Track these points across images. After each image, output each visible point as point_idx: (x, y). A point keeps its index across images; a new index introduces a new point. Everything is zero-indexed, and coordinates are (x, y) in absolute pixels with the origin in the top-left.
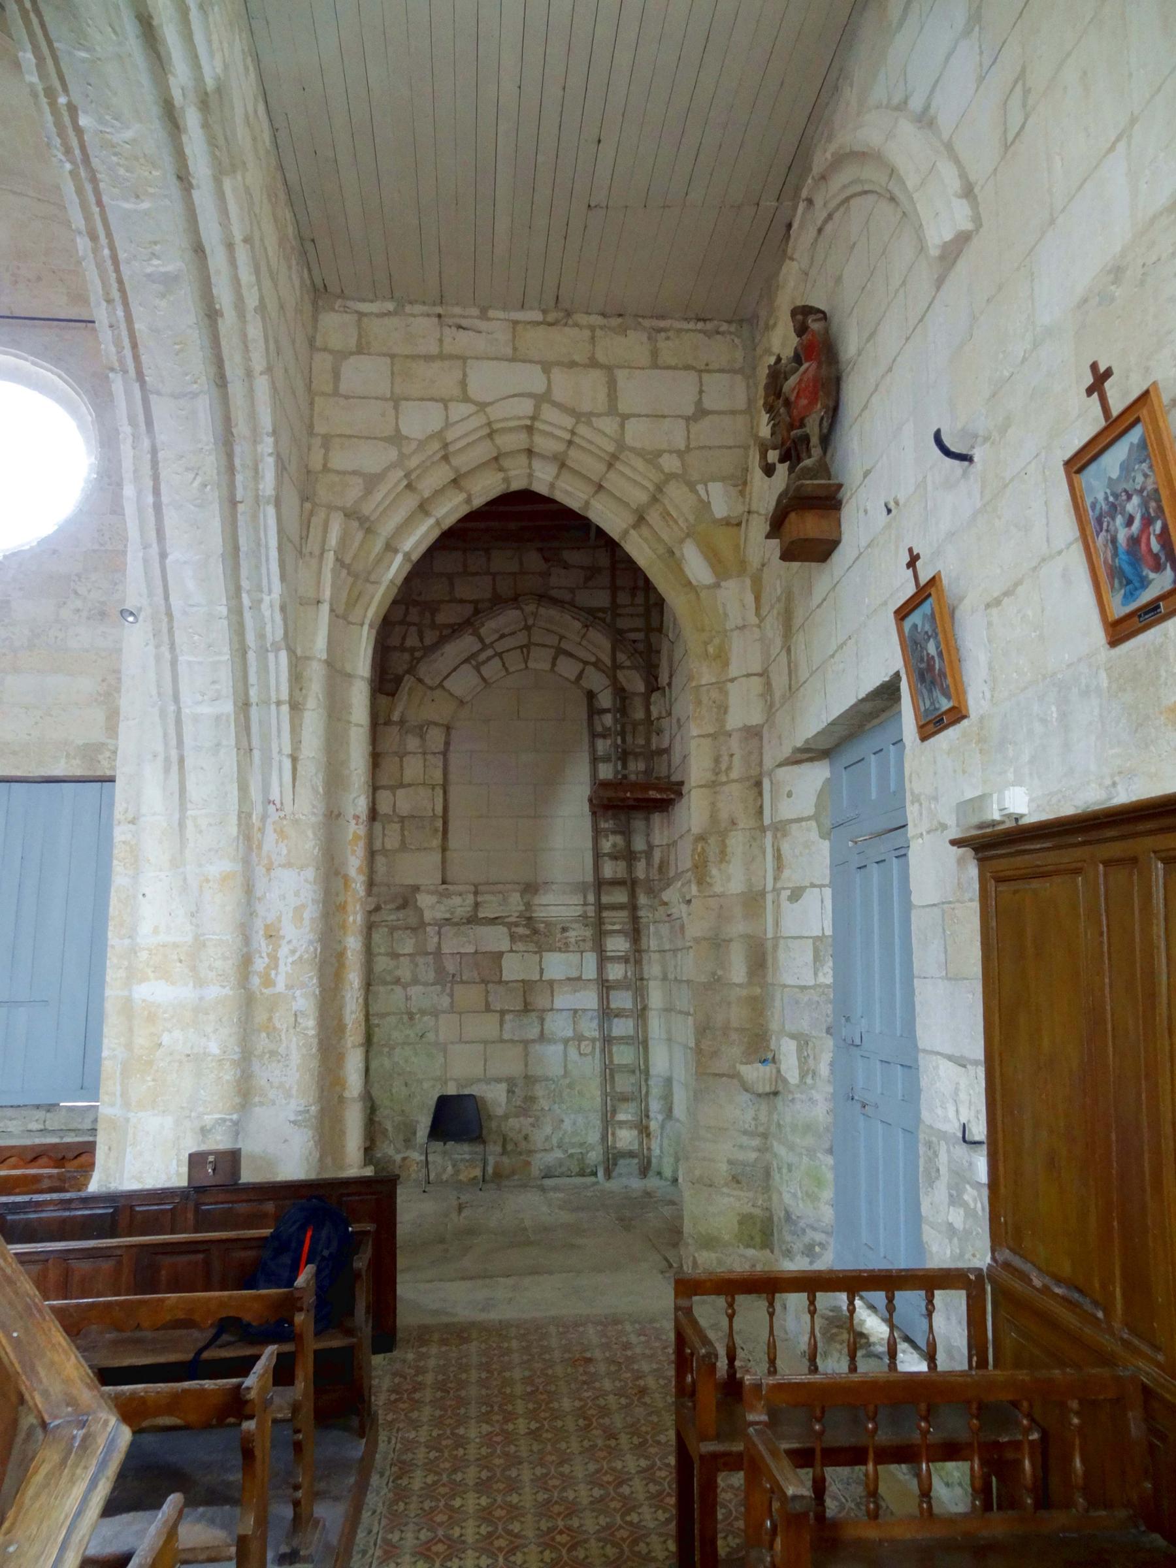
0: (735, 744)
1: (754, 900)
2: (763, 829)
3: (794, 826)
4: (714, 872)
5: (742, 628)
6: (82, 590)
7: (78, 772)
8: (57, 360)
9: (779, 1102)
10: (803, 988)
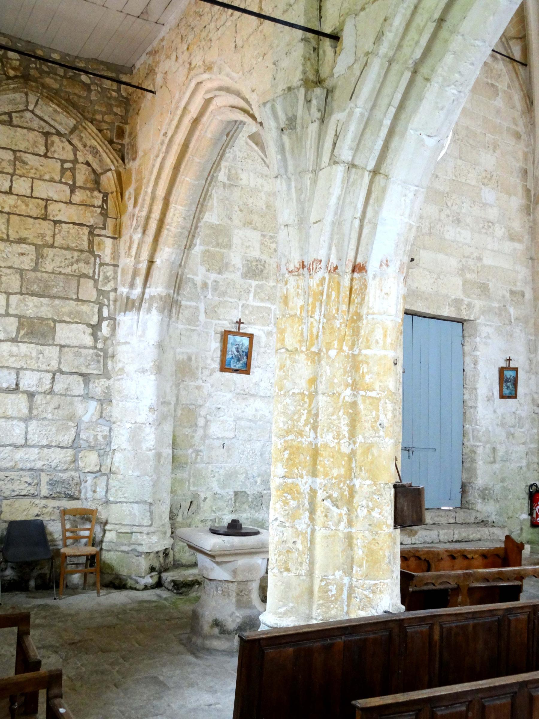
6: (449, 204)
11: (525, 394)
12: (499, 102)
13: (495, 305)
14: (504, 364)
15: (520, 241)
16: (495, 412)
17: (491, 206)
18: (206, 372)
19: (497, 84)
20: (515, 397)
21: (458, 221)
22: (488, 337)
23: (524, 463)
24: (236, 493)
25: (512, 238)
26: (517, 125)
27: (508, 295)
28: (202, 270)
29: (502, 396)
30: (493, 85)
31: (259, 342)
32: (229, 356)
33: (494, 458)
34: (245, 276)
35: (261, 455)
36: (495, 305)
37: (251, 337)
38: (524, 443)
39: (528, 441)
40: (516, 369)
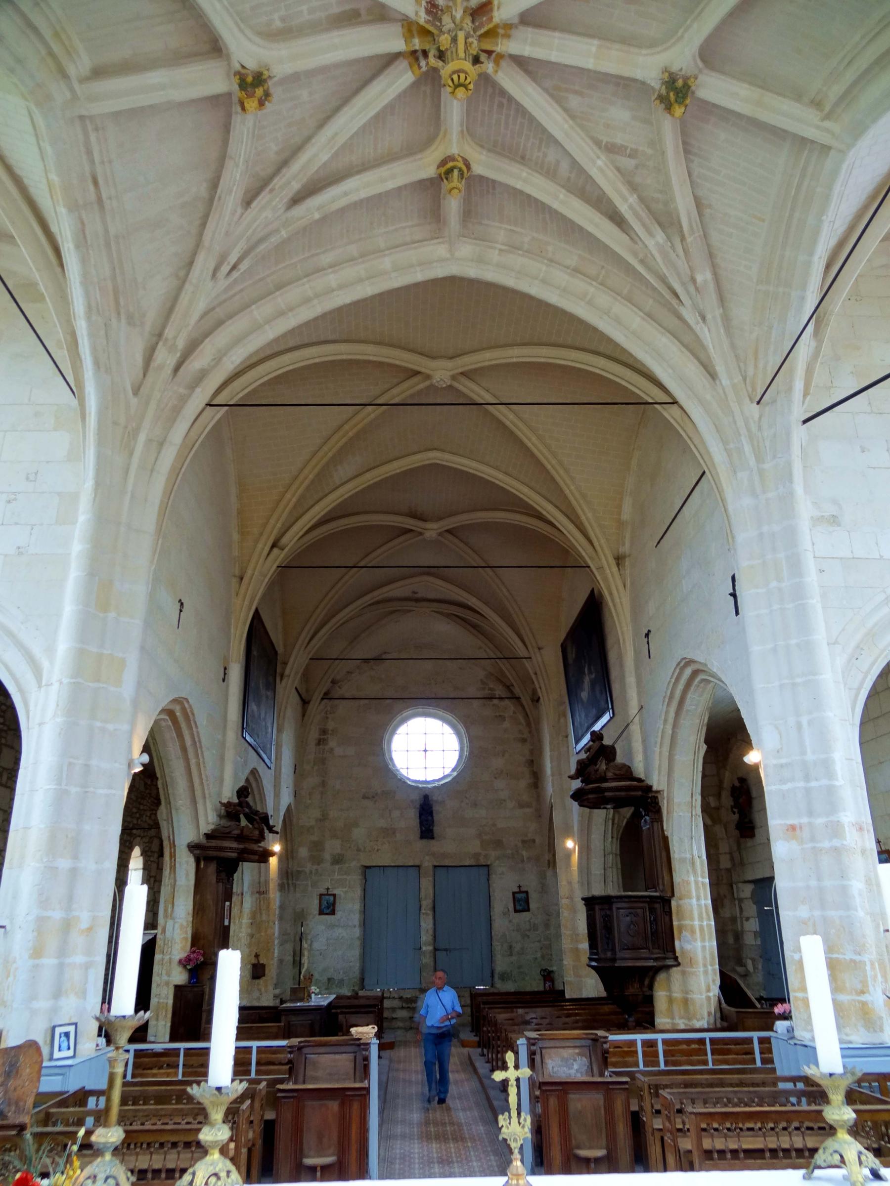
1: (734, 920)
2: (735, 899)
3: (745, 900)
4: (720, 910)
7: (474, 864)
8: (451, 711)
9: (748, 978)
10: (752, 945)
12: (507, 724)
14: (517, 890)
15: (528, 805)
16: (510, 921)
17: (502, 790)
20: (528, 910)
21: (475, 805)
22: (503, 873)
23: (539, 955)
24: (329, 980)
25: (521, 805)
26: (523, 734)
27: (520, 844)
28: (309, 865)
29: (516, 911)
30: (500, 716)
31: (340, 898)
32: (323, 907)
36: (509, 851)
37: (334, 895)
38: (539, 941)
39: (542, 939)
40: (527, 892)
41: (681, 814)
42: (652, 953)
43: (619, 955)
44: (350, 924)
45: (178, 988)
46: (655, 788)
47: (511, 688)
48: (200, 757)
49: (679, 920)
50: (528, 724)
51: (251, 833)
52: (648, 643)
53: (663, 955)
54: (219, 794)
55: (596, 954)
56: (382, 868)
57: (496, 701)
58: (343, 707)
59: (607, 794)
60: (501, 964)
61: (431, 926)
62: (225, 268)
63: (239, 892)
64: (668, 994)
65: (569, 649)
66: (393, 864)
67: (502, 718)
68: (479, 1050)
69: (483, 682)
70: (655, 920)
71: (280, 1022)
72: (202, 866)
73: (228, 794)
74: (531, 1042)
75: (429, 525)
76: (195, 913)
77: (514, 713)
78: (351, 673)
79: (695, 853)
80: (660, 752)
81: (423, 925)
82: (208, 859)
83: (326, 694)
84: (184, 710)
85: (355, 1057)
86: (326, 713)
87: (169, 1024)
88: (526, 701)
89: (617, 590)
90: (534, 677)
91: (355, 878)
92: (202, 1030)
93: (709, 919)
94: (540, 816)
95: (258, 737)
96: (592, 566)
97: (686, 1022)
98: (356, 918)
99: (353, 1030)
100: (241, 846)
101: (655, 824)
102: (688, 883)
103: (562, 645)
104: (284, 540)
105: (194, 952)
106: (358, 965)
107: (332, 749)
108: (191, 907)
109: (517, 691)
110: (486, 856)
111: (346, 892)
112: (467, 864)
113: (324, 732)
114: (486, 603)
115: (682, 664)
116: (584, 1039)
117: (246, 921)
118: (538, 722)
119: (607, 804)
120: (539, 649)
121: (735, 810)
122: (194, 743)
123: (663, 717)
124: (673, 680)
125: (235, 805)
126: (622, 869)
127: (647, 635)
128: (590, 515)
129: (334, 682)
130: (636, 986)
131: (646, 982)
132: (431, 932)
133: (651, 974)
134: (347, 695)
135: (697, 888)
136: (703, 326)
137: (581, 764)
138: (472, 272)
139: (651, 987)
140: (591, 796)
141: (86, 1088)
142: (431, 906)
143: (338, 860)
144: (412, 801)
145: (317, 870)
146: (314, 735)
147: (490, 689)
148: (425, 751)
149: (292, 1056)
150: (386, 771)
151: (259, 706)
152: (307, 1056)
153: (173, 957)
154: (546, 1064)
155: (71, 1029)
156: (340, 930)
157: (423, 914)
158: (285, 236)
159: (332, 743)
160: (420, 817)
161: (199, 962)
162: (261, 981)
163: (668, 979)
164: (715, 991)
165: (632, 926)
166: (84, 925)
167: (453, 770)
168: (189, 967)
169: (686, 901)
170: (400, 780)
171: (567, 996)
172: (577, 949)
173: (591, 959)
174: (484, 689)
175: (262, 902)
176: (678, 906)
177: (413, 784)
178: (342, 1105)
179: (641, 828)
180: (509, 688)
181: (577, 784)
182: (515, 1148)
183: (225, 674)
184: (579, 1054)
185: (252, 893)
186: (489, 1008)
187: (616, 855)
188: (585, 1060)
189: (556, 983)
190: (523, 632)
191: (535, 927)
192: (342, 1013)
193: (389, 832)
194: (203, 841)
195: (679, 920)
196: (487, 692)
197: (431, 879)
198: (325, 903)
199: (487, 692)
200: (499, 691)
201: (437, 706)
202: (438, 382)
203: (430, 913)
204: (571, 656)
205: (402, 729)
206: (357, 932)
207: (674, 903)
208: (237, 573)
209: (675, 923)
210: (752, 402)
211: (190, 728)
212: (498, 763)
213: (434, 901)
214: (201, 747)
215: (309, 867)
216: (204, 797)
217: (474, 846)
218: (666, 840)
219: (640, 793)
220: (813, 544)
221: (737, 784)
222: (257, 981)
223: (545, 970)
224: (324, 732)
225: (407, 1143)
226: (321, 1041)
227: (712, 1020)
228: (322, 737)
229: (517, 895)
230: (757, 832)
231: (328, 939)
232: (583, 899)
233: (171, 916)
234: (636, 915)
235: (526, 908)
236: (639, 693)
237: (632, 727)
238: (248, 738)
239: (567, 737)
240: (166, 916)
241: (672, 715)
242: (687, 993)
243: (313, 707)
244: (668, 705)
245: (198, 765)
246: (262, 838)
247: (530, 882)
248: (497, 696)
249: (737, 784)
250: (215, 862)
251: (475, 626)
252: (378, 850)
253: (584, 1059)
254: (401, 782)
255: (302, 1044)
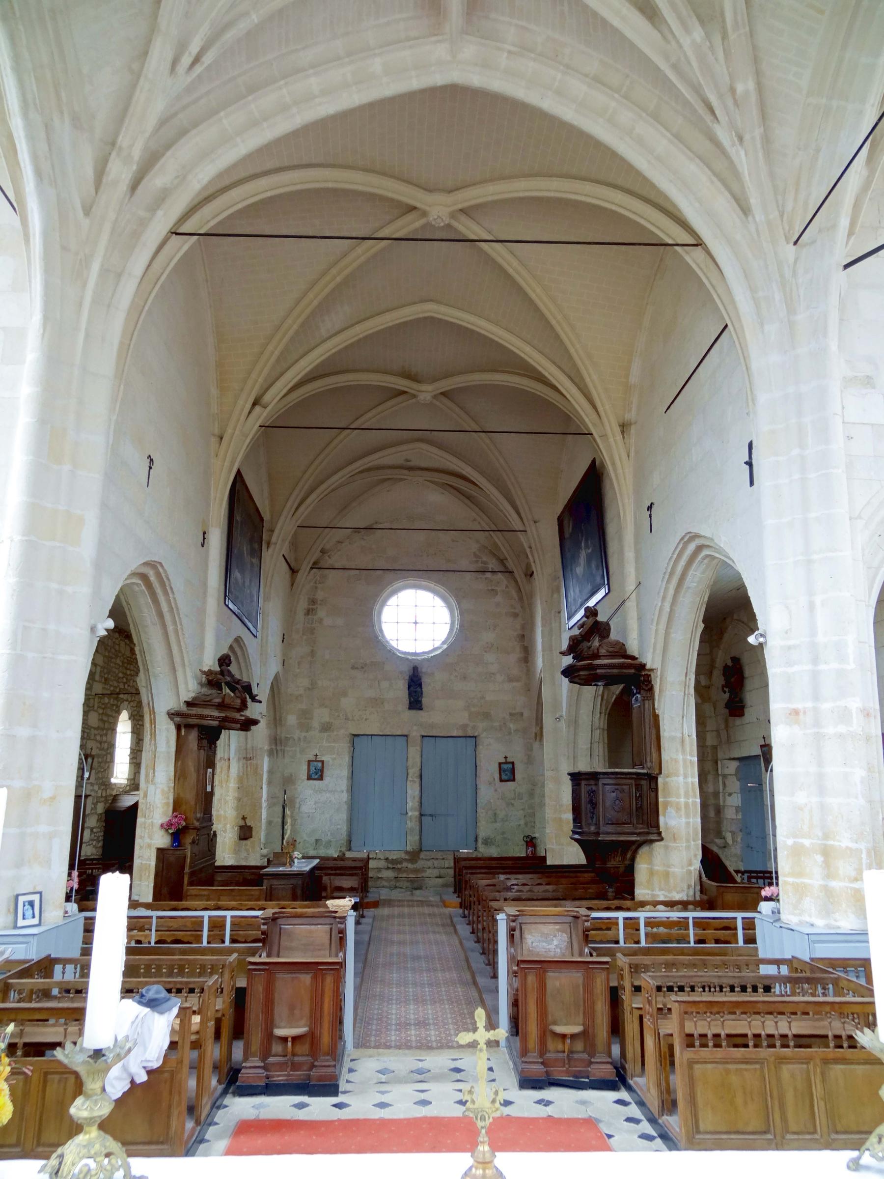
0: (709, 750)
1: (716, 794)
5: (710, 717)
9: (726, 849)
10: (733, 819)
11: (524, 778)
12: (499, 598)
13: (496, 724)
14: (504, 760)
15: (518, 681)
16: (496, 790)
17: (492, 664)
18: (300, 781)
19: (496, 588)
20: (514, 780)
21: (464, 678)
23: (522, 822)
24: (317, 841)
25: (510, 680)
26: (515, 608)
27: (508, 717)
29: (501, 780)
30: (493, 590)
33: (495, 819)
34: (321, 731)
35: (330, 820)
36: (496, 724)
37: (323, 762)
38: (523, 809)
40: (513, 763)
41: (674, 693)
42: (636, 828)
43: (603, 829)
44: (339, 790)
45: (160, 851)
46: (648, 667)
47: (505, 561)
48: (178, 624)
49: (665, 797)
50: (521, 599)
51: (233, 701)
52: (650, 516)
53: (646, 830)
54: (200, 662)
55: (580, 827)
56: (370, 737)
57: (488, 575)
58: (332, 576)
59: (598, 671)
60: (484, 830)
61: (417, 793)
62: (186, 60)
63: (226, 757)
64: (649, 866)
65: (566, 522)
66: (381, 734)
67: (494, 592)
68: (461, 911)
69: (475, 555)
70: (640, 796)
71: (262, 886)
72: (183, 734)
73: (210, 662)
74: (512, 919)
75: (424, 387)
76: (177, 778)
77: (507, 587)
78: (342, 542)
79: (686, 732)
80: (657, 630)
81: (409, 791)
82: (189, 727)
83: (314, 563)
84: (158, 575)
85: (331, 929)
86: (316, 583)
87: (152, 885)
88: (519, 574)
89: (620, 459)
90: (528, 550)
91: (344, 747)
92: (184, 891)
93: (695, 797)
94: (529, 690)
95: (243, 606)
96: (595, 435)
97: (666, 894)
98: (344, 784)
99: (329, 903)
100: (223, 715)
101: (647, 702)
102: (676, 761)
103: (559, 518)
104: (267, 398)
105: (176, 817)
106: (345, 828)
107: (321, 621)
108: (173, 774)
109: (511, 565)
110: (474, 728)
111: (335, 759)
112: (454, 735)
113: (313, 602)
114: (482, 473)
115: (685, 539)
116: (567, 916)
117: (233, 784)
118: (531, 596)
119: (599, 681)
120: (535, 522)
121: (725, 689)
122: (171, 609)
123: (662, 594)
124: (675, 556)
125: (216, 673)
126: (609, 743)
127: (650, 508)
128: (595, 377)
129: (323, 551)
130: (618, 858)
131: (629, 855)
132: (417, 799)
133: (634, 847)
134: (337, 565)
135: (685, 767)
136: (739, 148)
137: (573, 640)
138: (476, 79)
139: (633, 859)
140: (581, 673)
141: (52, 956)
142: (418, 773)
143: (326, 728)
144: (401, 673)
145: (305, 737)
146: (303, 605)
147: (483, 562)
148: (416, 623)
149: (266, 927)
150: (376, 641)
151: (242, 572)
152: (282, 926)
153: (155, 821)
154: (525, 938)
155: (36, 898)
156: (328, 795)
157: (410, 781)
158: (256, 21)
159: (321, 613)
160: (409, 687)
161: (180, 827)
162: (248, 842)
163: (651, 853)
164: (697, 865)
165: (617, 802)
166: (47, 795)
167: (444, 643)
168: (171, 831)
169: (674, 779)
170: (390, 651)
171: (548, 863)
172: (560, 819)
173: (574, 832)
174: (477, 562)
175: (249, 767)
176: (665, 784)
177: (403, 656)
178: (315, 978)
179: (632, 706)
180: (502, 561)
181: (568, 660)
182: (482, 1128)
183: (204, 538)
184: (558, 930)
185: (239, 759)
186: (472, 873)
187: (603, 729)
188: (565, 937)
189: (538, 849)
190: (518, 503)
191: (520, 796)
192: (326, 875)
193: (376, 702)
194: (184, 708)
195: (665, 797)
196: (480, 565)
197: (419, 748)
198: (313, 769)
199: (480, 566)
200: (493, 564)
201: (429, 579)
202: (435, 219)
203: (418, 780)
204: (568, 530)
205: (393, 601)
206: (345, 797)
207: (660, 780)
208: (216, 431)
209: (661, 800)
210: (788, 243)
211: (166, 593)
212: (488, 637)
213: (421, 770)
214: (179, 614)
215: (297, 734)
216: (184, 665)
217: (462, 718)
218: (656, 718)
219: (633, 671)
220: (843, 408)
221: (730, 663)
222: (245, 842)
223: (527, 837)
224: (313, 602)
225: (385, 1004)
226: (296, 913)
227: (691, 893)
228: (311, 607)
229: (503, 766)
230: (746, 711)
231: (316, 803)
232: (569, 774)
233: (152, 781)
234: (622, 791)
235: (512, 778)
236: (637, 569)
237: (627, 604)
238: (231, 605)
239: (559, 612)
240: (147, 781)
241: (671, 592)
242: (669, 866)
243: (301, 577)
244: (668, 582)
245: (176, 631)
246: (244, 706)
247: (517, 755)
248: (490, 570)
249: (730, 663)
250: (196, 729)
251: (469, 497)
252: (366, 720)
253: (564, 935)
254: (391, 653)
255: (276, 915)
